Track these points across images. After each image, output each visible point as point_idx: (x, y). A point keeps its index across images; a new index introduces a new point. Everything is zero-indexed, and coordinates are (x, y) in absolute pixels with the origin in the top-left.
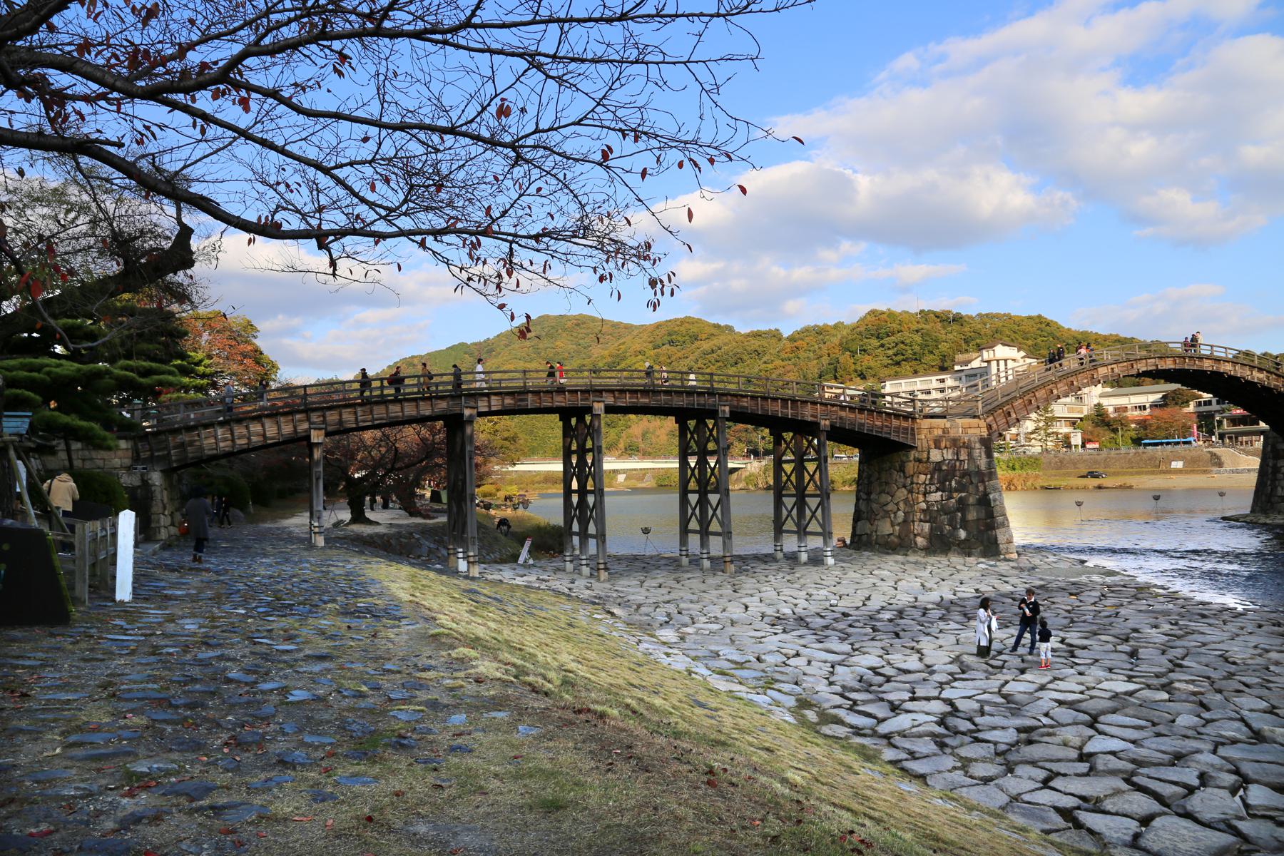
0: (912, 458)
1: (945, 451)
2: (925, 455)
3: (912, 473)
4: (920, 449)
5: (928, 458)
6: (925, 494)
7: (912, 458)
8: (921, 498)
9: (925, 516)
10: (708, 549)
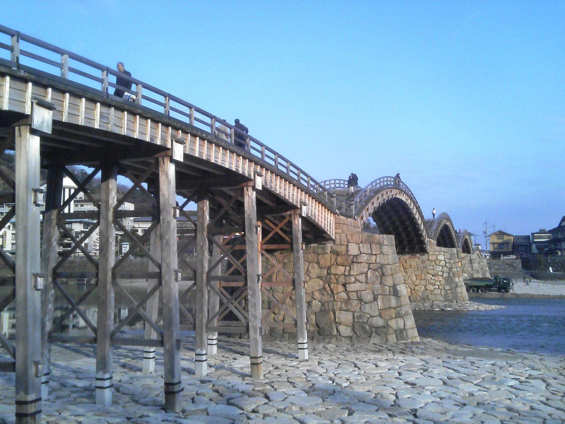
0: (329, 250)
1: (361, 245)
2: (344, 248)
3: (328, 264)
4: (338, 242)
5: (347, 251)
6: (344, 285)
7: (329, 250)
8: (341, 288)
9: (346, 305)
10: (207, 351)
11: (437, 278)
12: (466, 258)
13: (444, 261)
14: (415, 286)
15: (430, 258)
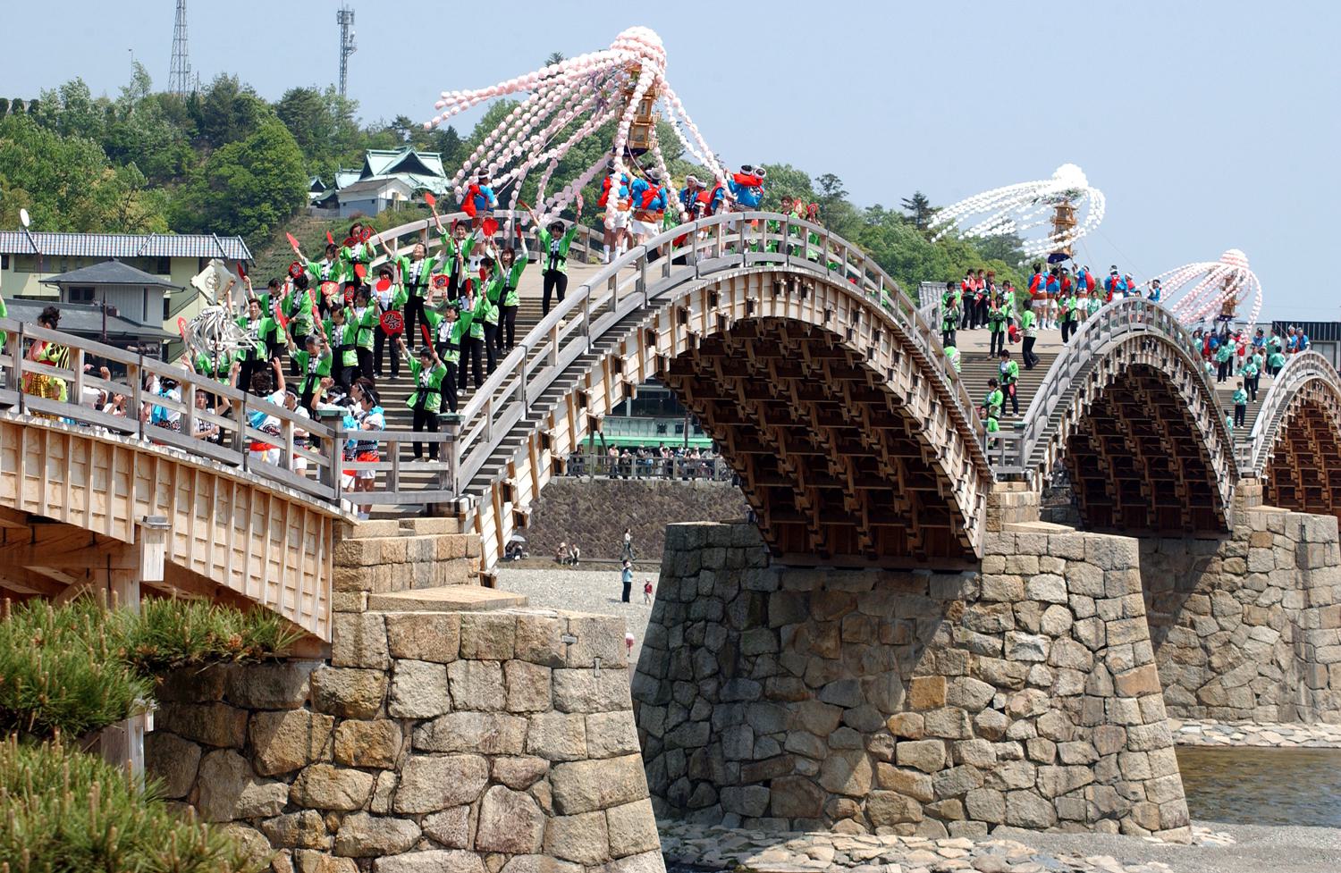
11: (1018, 703)
12: (1278, 539)
13: (1067, 605)
14: (901, 739)
15: (989, 593)
